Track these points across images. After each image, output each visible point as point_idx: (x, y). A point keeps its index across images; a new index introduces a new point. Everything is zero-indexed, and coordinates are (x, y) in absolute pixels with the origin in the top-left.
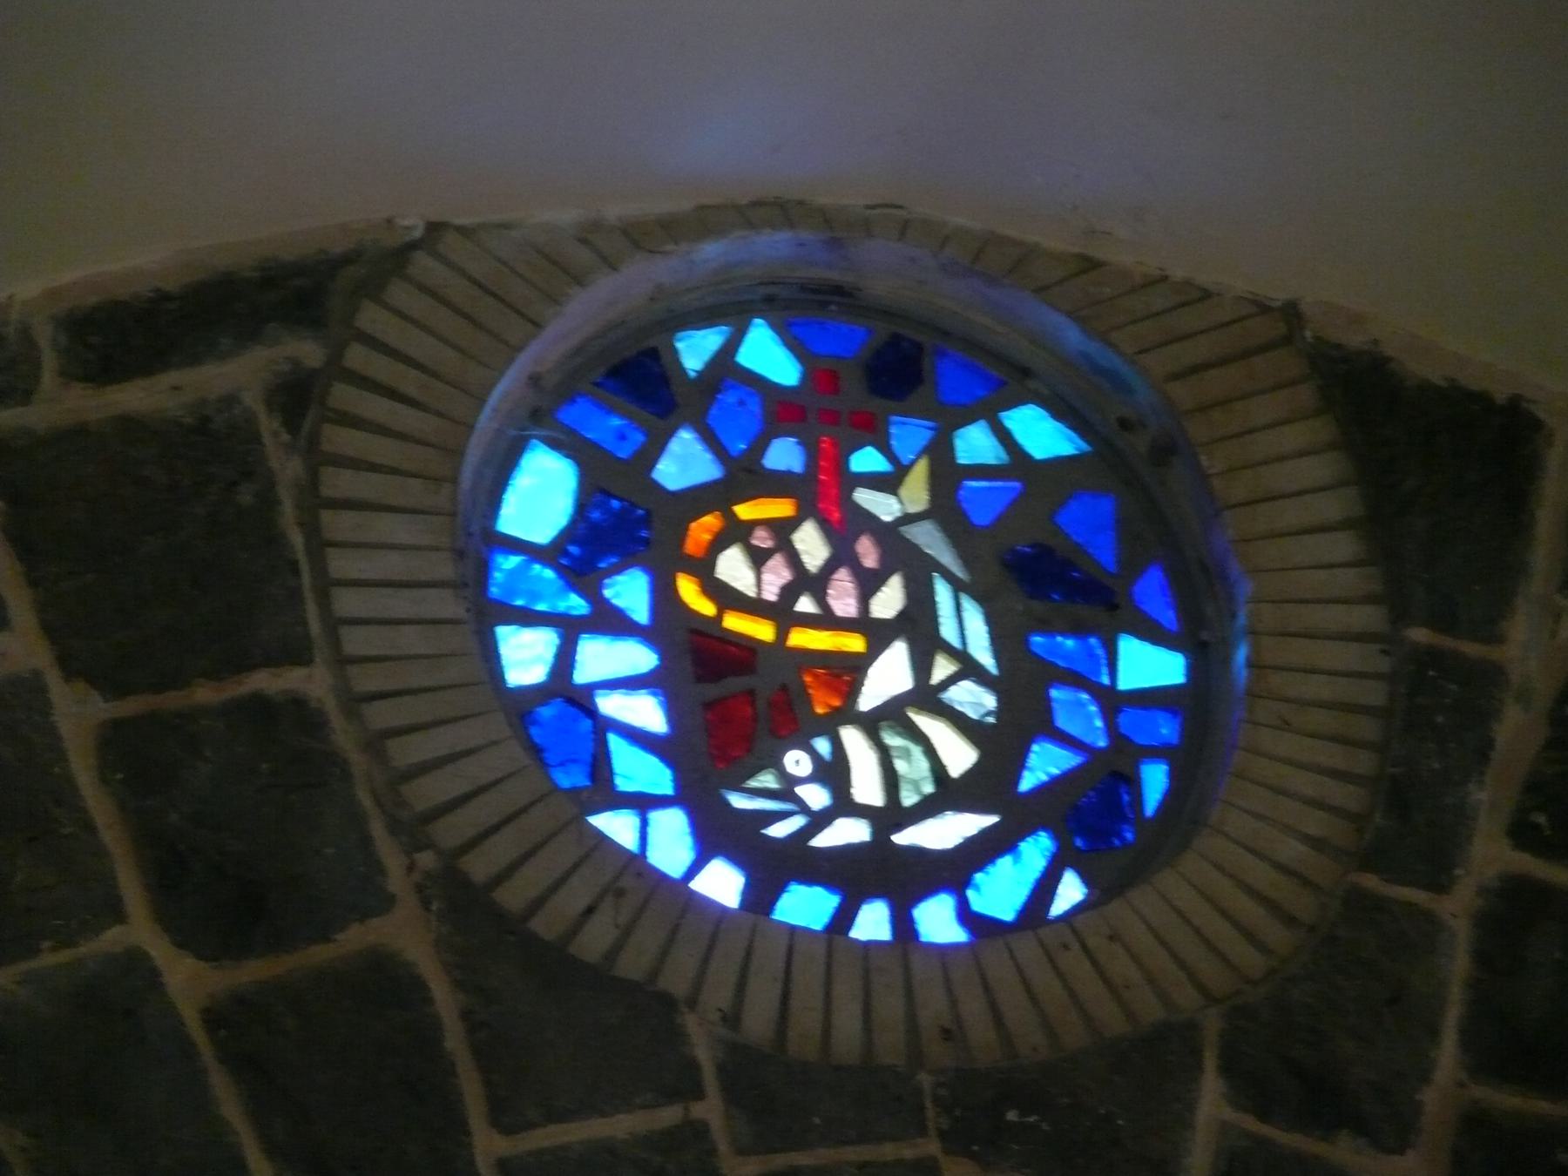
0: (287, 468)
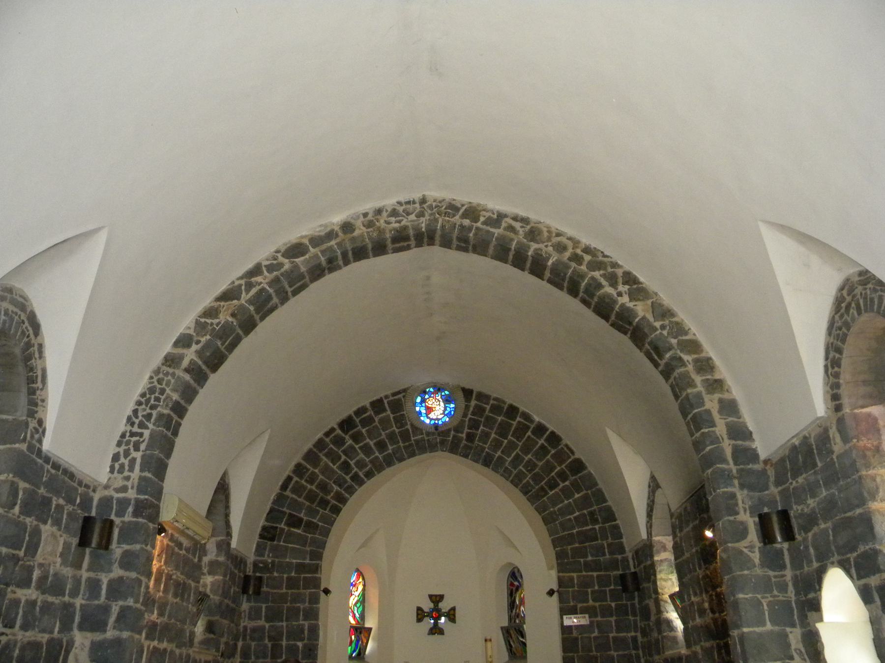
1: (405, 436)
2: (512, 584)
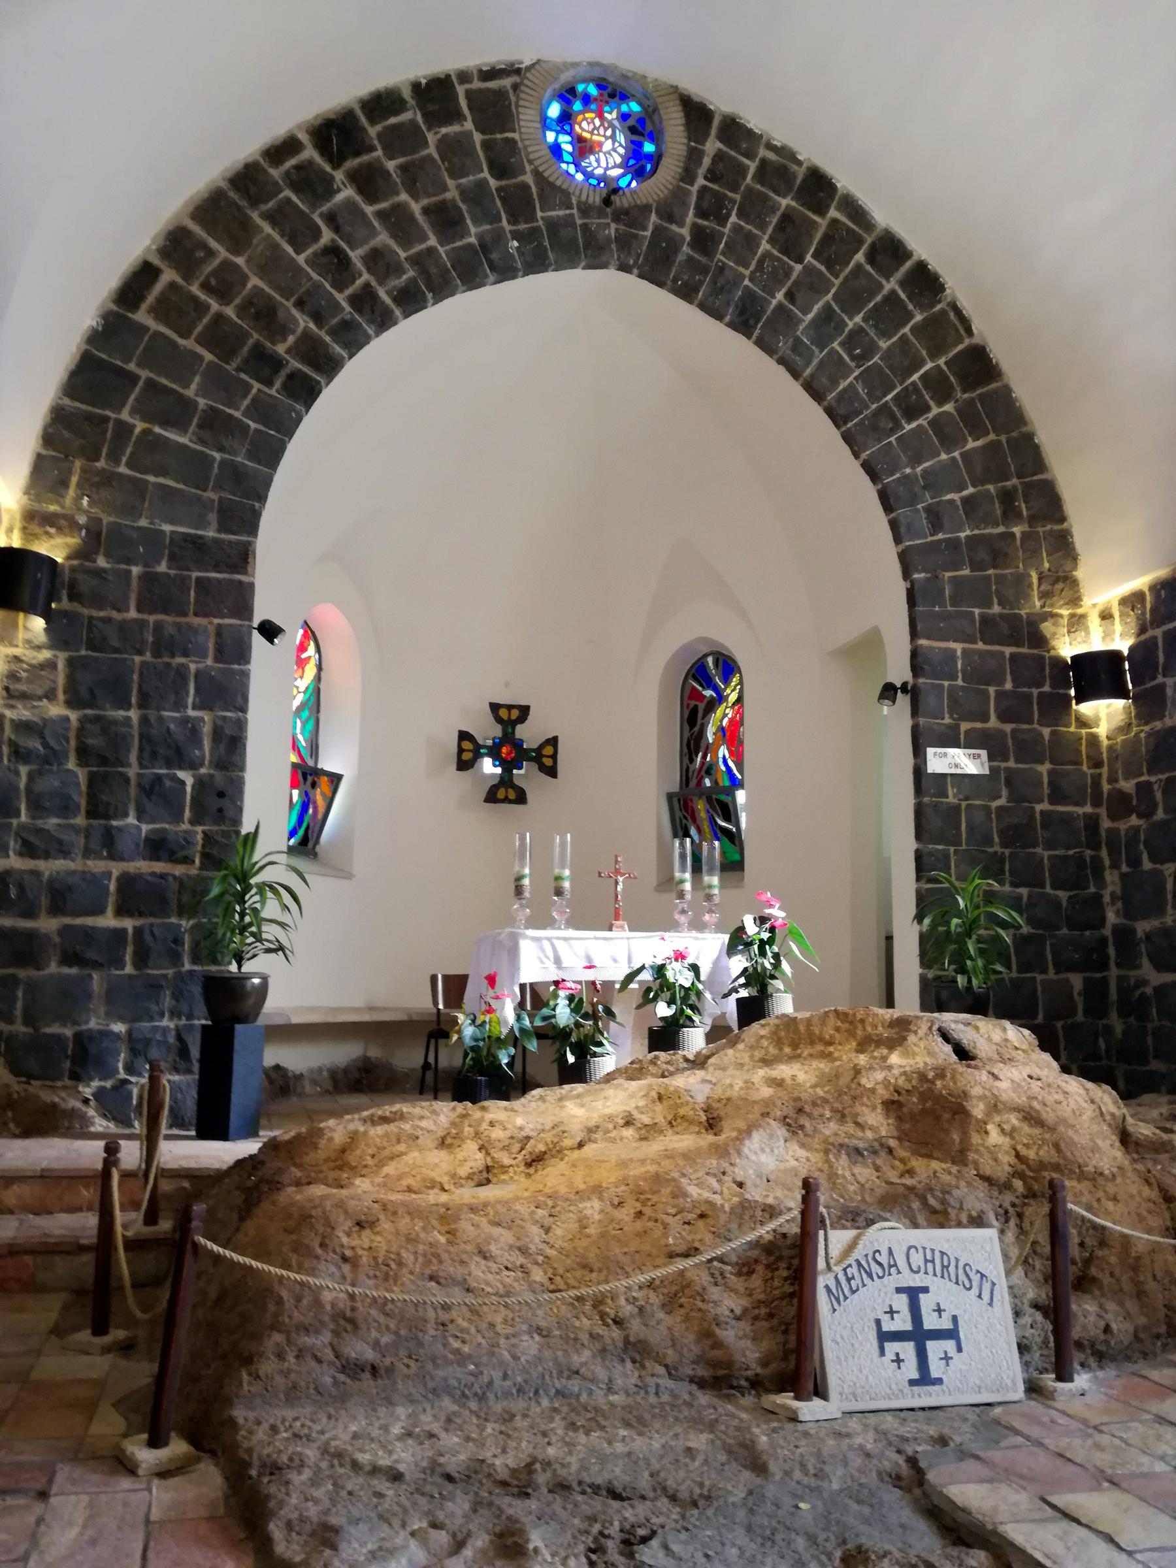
0: (513, 99)
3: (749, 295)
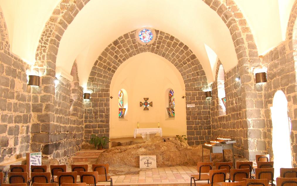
1: (136, 47)
2: (170, 95)
3: (164, 53)
